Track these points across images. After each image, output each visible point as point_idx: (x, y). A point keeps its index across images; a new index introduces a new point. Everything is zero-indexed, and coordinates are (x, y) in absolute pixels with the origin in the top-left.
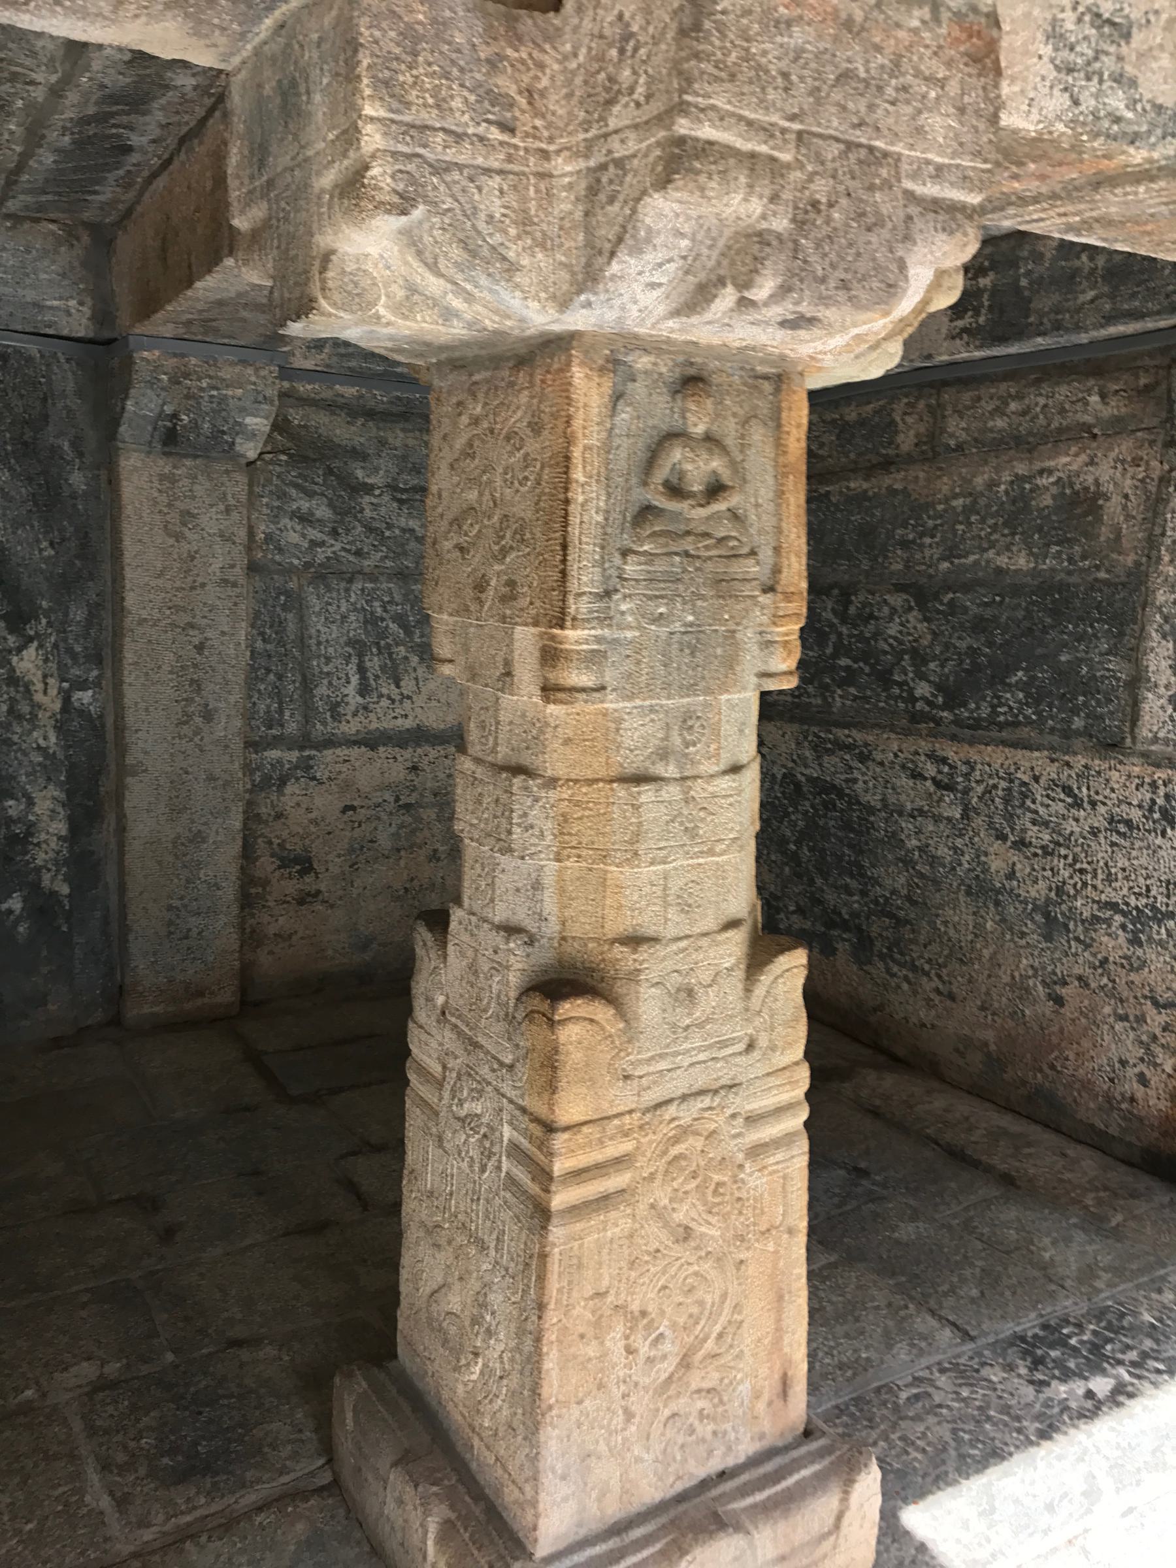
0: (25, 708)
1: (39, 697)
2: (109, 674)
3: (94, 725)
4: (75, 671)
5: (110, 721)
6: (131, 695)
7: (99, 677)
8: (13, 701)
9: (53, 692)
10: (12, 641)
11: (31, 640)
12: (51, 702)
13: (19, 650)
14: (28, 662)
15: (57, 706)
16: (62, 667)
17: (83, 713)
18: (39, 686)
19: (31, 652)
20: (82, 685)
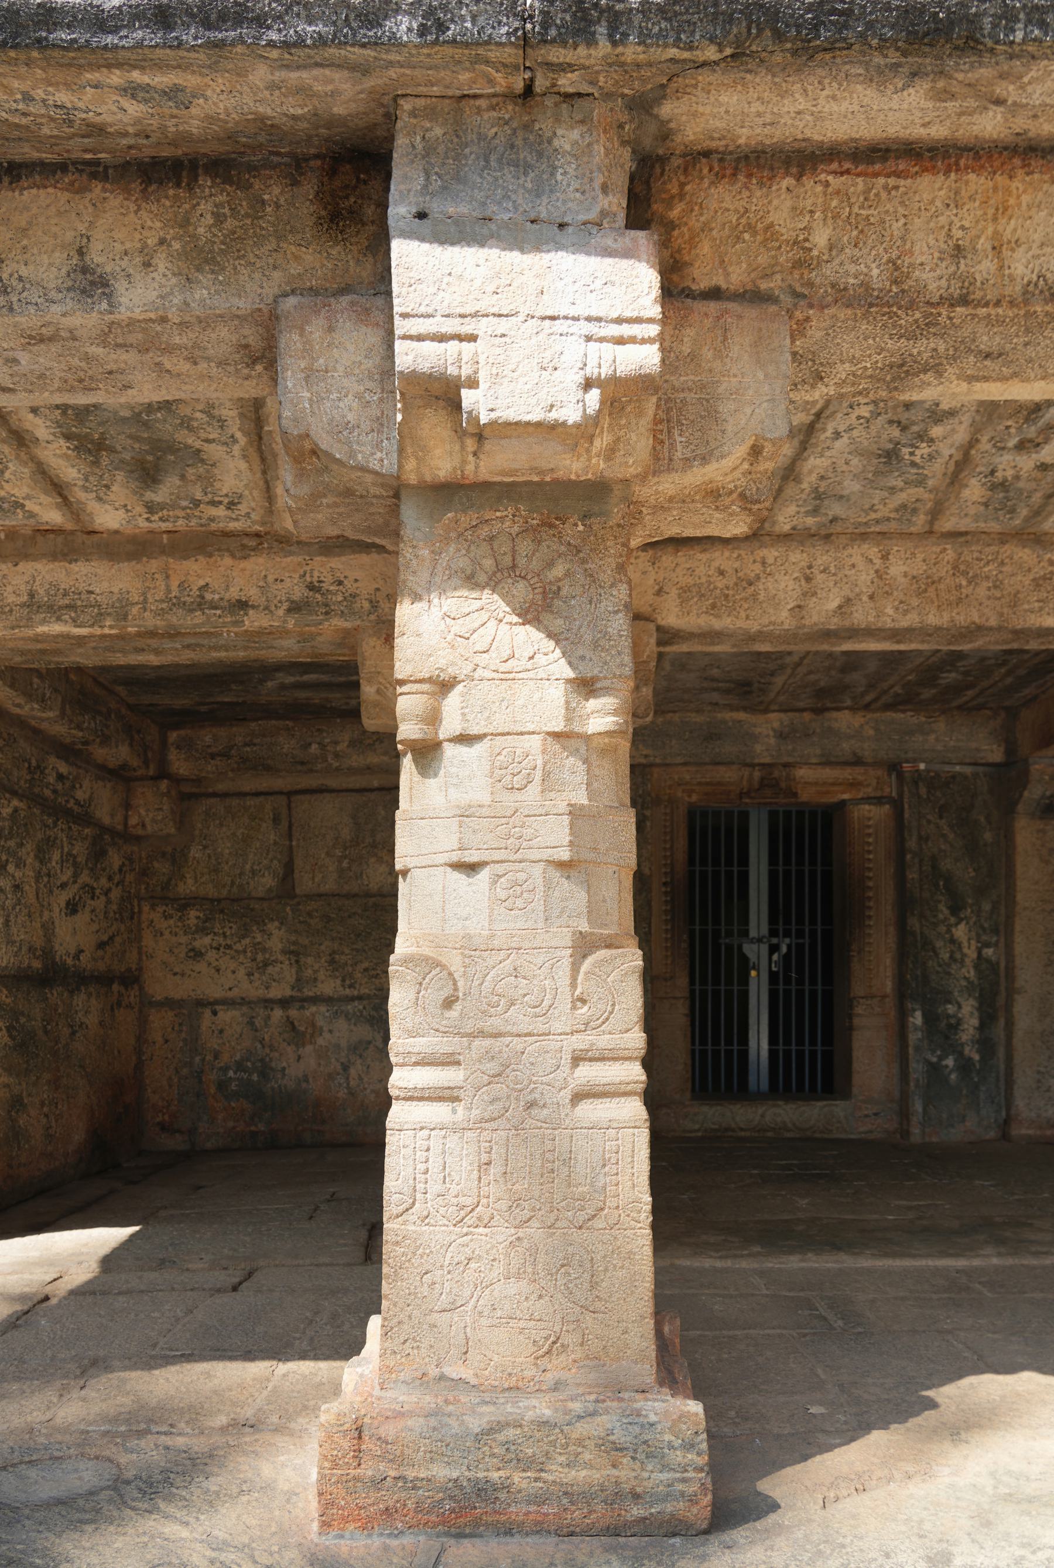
0: (958, 956)
1: (966, 950)
2: (1002, 940)
3: (994, 967)
4: (984, 938)
5: (1003, 965)
6: (1019, 948)
7: (997, 941)
8: (952, 952)
9: (973, 948)
10: (953, 920)
11: (962, 920)
12: (971, 953)
13: (957, 925)
14: (961, 932)
15: (975, 955)
16: (978, 936)
17: (988, 961)
18: (966, 944)
19: (962, 927)
20: (987, 945)
